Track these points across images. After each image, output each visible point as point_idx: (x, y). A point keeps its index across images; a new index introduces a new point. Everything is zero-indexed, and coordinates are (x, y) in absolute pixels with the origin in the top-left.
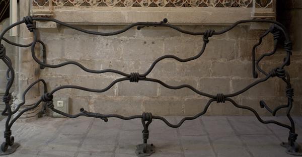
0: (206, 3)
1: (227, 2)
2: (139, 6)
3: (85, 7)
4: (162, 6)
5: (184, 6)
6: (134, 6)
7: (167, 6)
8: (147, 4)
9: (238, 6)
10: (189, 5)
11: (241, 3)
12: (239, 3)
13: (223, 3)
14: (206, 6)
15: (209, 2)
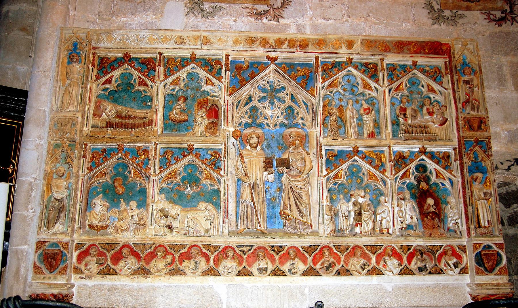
0: (381, 267)
1: (420, 264)
2: (250, 274)
3: (140, 278)
4: (294, 274)
5: (338, 273)
6: (239, 274)
7: (305, 274)
8: (265, 269)
9: (441, 272)
10: (348, 271)
11: (445, 266)
12: (442, 266)
13: (413, 266)
14: (379, 273)
15: (385, 266)
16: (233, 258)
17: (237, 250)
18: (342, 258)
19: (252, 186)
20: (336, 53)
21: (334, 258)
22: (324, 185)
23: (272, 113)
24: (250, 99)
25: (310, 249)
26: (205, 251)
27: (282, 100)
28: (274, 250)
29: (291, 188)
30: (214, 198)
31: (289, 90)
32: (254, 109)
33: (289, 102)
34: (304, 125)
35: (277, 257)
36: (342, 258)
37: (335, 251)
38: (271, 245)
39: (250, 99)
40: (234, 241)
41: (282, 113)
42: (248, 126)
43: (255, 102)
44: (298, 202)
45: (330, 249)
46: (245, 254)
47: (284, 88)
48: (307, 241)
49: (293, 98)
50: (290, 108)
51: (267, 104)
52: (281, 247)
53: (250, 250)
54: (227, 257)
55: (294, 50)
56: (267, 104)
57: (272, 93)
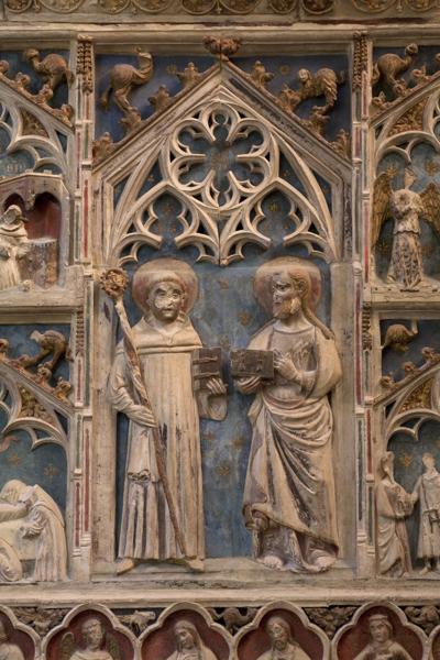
16: (103, 645)
17: (116, 622)
18: (427, 642)
19: (161, 435)
20: (420, 21)
21: (402, 643)
22: (376, 429)
23: (223, 212)
24: (156, 172)
25: (330, 613)
26: (18, 624)
27: (253, 173)
28: (221, 621)
29: (277, 437)
30: (50, 467)
31: (273, 140)
32: (168, 200)
33: (272, 177)
34: (316, 246)
35: (232, 641)
36: (427, 642)
37: (406, 623)
38: (213, 606)
39: (156, 172)
40: (105, 595)
41: (253, 213)
42: (148, 251)
43: (172, 180)
44: (296, 479)
45: (392, 617)
46: (137, 634)
47: (255, 137)
48: (322, 594)
49: (285, 167)
50: (275, 197)
51: (206, 184)
52: (243, 611)
53: (151, 622)
54: (82, 643)
55: (290, 18)
56: (206, 184)
57: (219, 149)
